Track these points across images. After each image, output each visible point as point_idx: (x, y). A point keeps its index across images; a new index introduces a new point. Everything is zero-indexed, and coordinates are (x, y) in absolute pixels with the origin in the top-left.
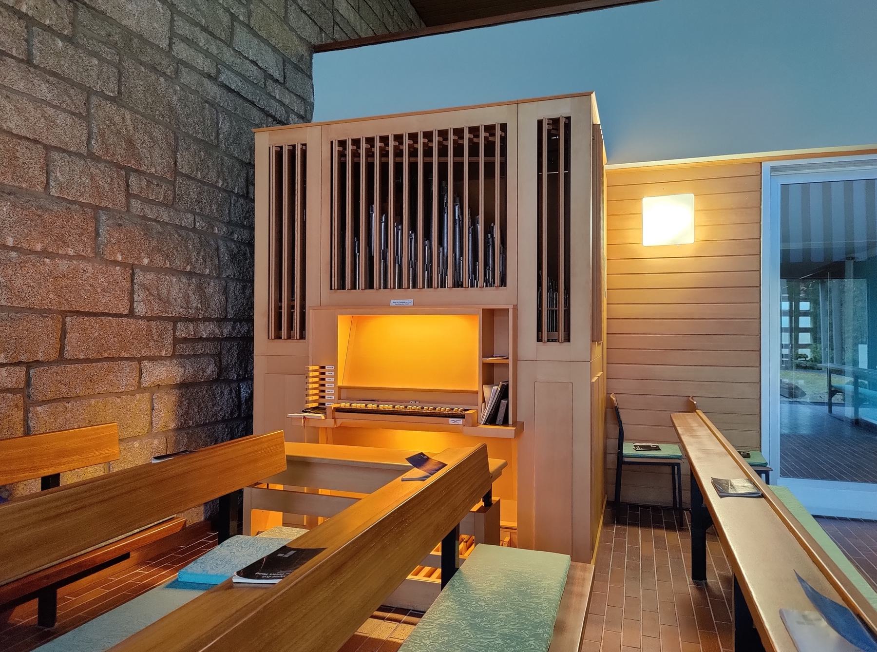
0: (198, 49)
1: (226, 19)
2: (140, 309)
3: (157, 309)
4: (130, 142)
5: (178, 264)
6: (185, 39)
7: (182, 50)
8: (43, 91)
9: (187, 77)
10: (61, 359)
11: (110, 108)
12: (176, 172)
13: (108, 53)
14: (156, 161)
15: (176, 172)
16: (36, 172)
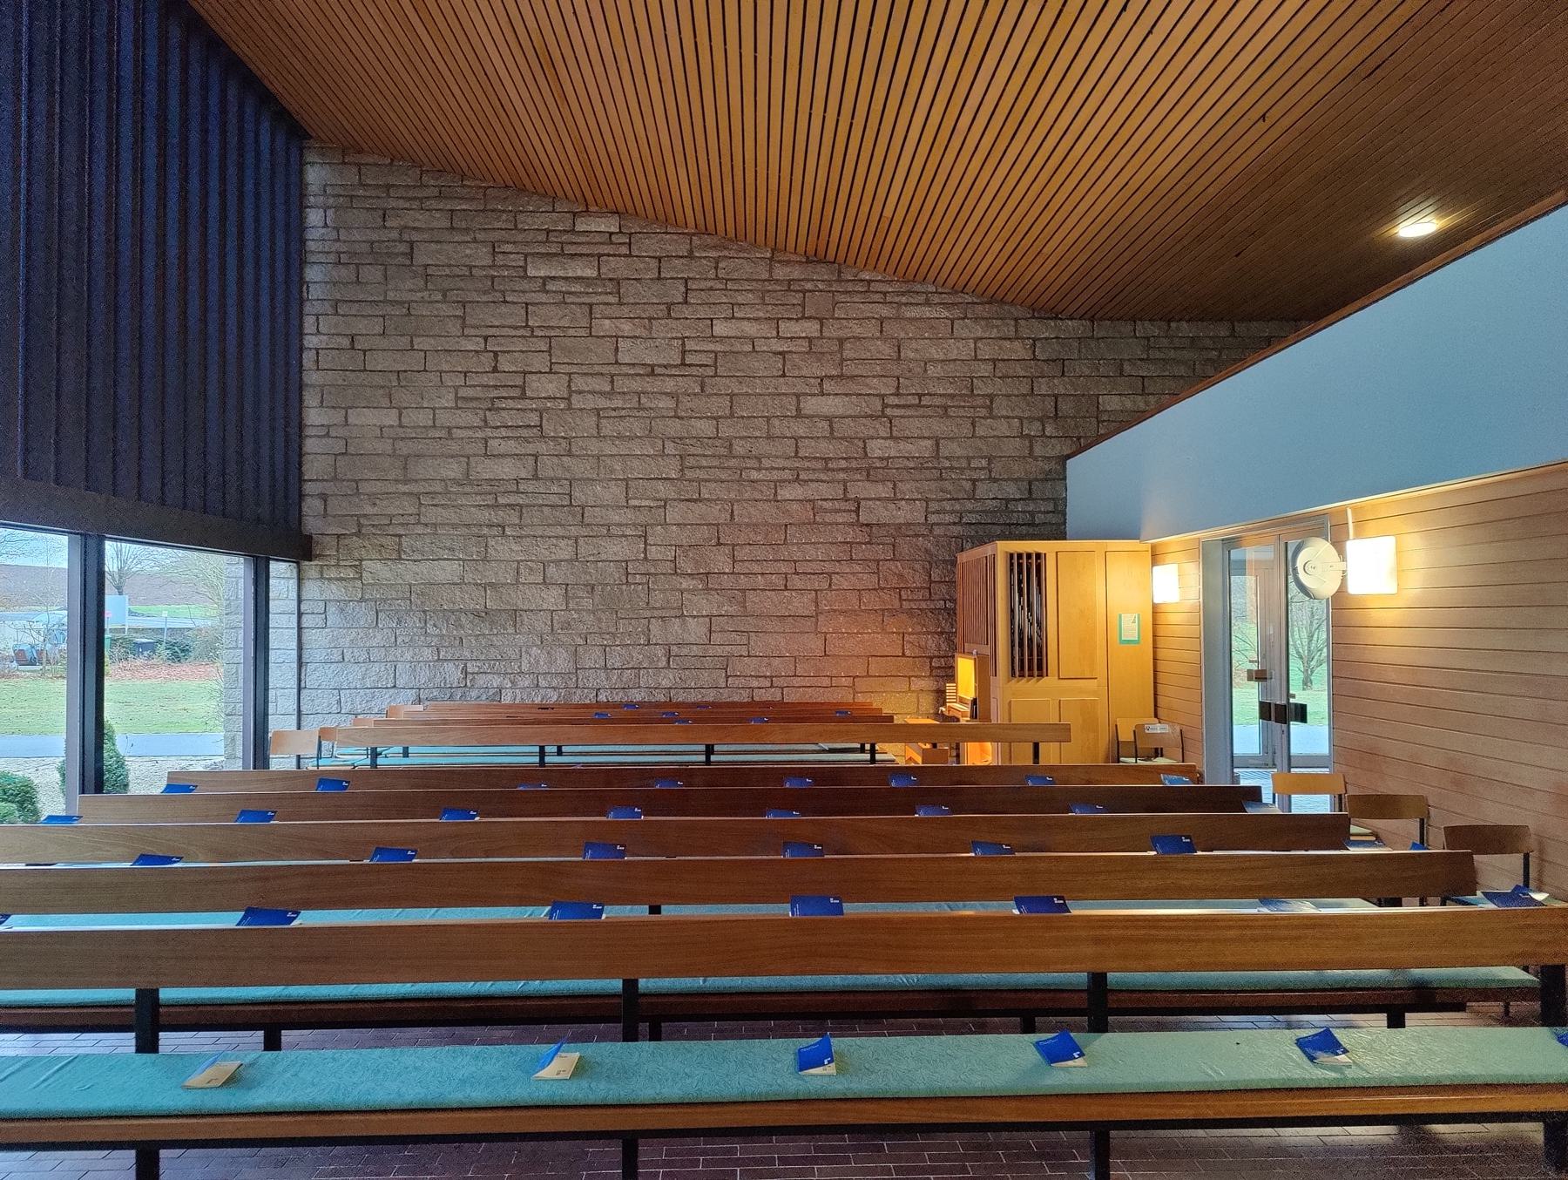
0: (945, 512)
1: (968, 486)
2: (907, 653)
3: (917, 652)
4: (901, 576)
5: (932, 629)
6: (938, 512)
7: (933, 518)
8: (858, 568)
9: (938, 531)
10: (868, 676)
11: (891, 565)
12: (931, 582)
13: (889, 540)
14: (918, 580)
15: (931, 582)
16: (855, 601)
